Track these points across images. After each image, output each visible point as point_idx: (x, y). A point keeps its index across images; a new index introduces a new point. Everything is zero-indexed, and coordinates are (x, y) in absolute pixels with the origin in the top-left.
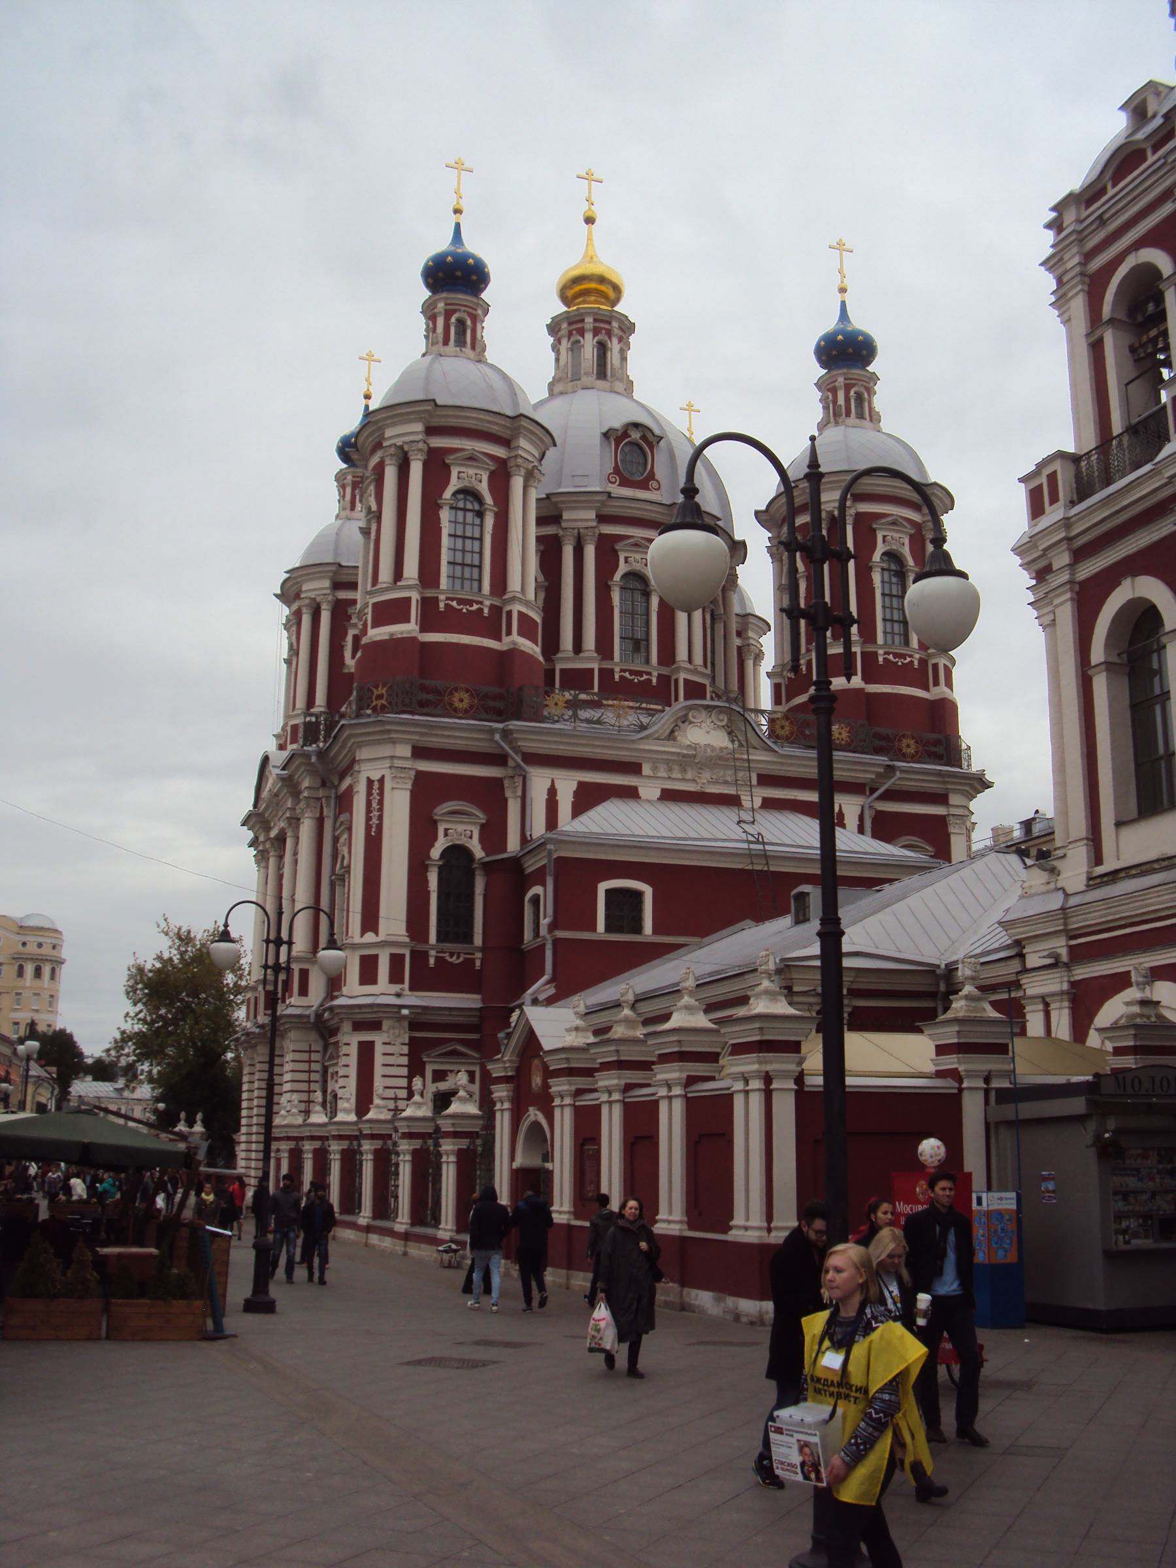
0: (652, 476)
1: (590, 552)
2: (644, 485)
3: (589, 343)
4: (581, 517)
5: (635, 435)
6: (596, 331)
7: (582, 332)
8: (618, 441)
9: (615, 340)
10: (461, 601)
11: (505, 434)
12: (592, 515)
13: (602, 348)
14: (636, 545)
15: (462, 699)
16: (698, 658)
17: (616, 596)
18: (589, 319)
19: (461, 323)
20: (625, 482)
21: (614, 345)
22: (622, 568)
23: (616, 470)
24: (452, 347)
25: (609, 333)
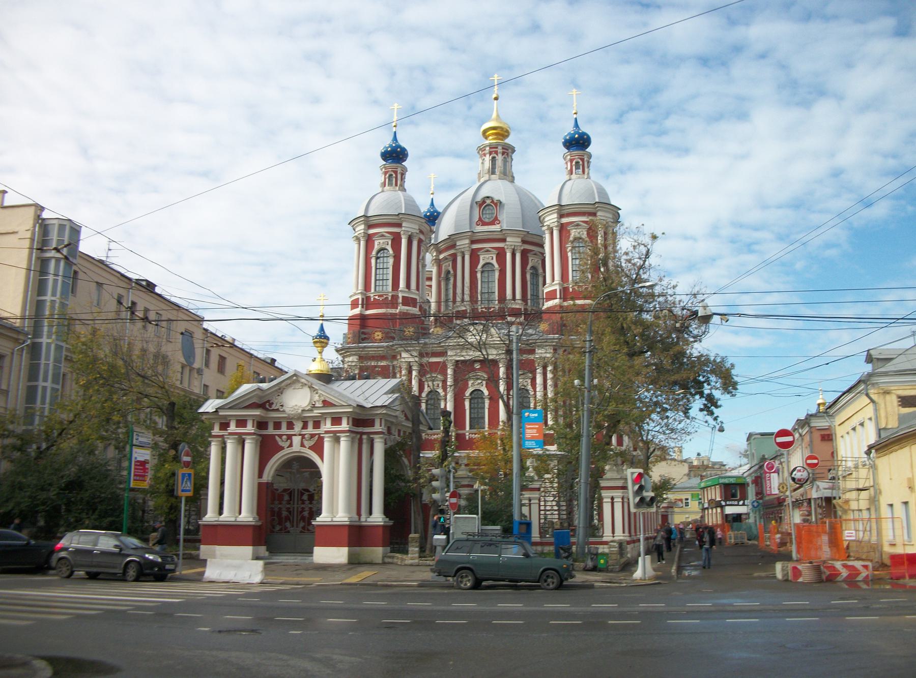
0: (496, 218)
1: (467, 258)
2: (492, 223)
3: (488, 158)
4: (463, 243)
5: (488, 202)
6: (490, 153)
7: (485, 155)
8: (480, 206)
9: (500, 155)
10: (379, 296)
11: (398, 222)
12: (467, 241)
13: (494, 158)
14: (488, 251)
15: (378, 335)
16: (518, 295)
17: (479, 275)
18: (488, 148)
19: (391, 175)
20: (484, 224)
21: (500, 158)
22: (482, 263)
23: (480, 219)
24: (387, 187)
25: (496, 153)
